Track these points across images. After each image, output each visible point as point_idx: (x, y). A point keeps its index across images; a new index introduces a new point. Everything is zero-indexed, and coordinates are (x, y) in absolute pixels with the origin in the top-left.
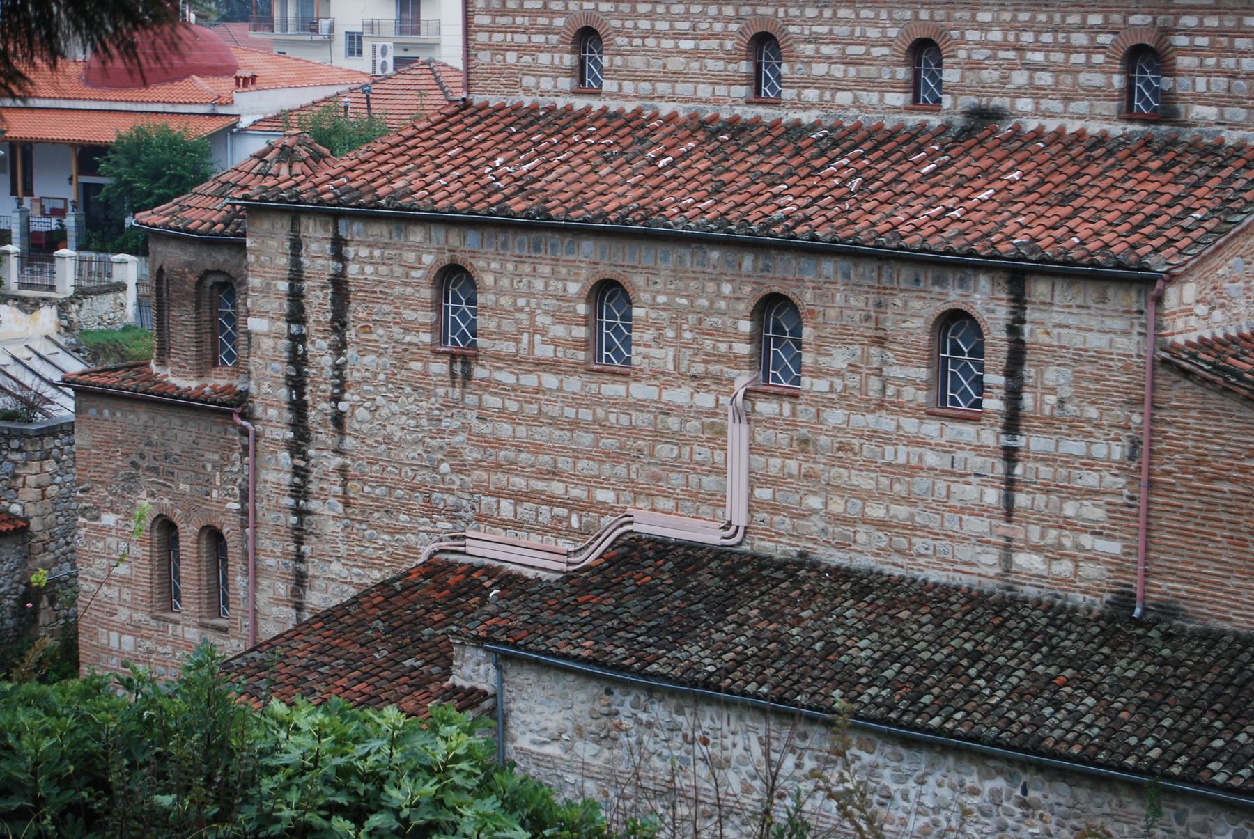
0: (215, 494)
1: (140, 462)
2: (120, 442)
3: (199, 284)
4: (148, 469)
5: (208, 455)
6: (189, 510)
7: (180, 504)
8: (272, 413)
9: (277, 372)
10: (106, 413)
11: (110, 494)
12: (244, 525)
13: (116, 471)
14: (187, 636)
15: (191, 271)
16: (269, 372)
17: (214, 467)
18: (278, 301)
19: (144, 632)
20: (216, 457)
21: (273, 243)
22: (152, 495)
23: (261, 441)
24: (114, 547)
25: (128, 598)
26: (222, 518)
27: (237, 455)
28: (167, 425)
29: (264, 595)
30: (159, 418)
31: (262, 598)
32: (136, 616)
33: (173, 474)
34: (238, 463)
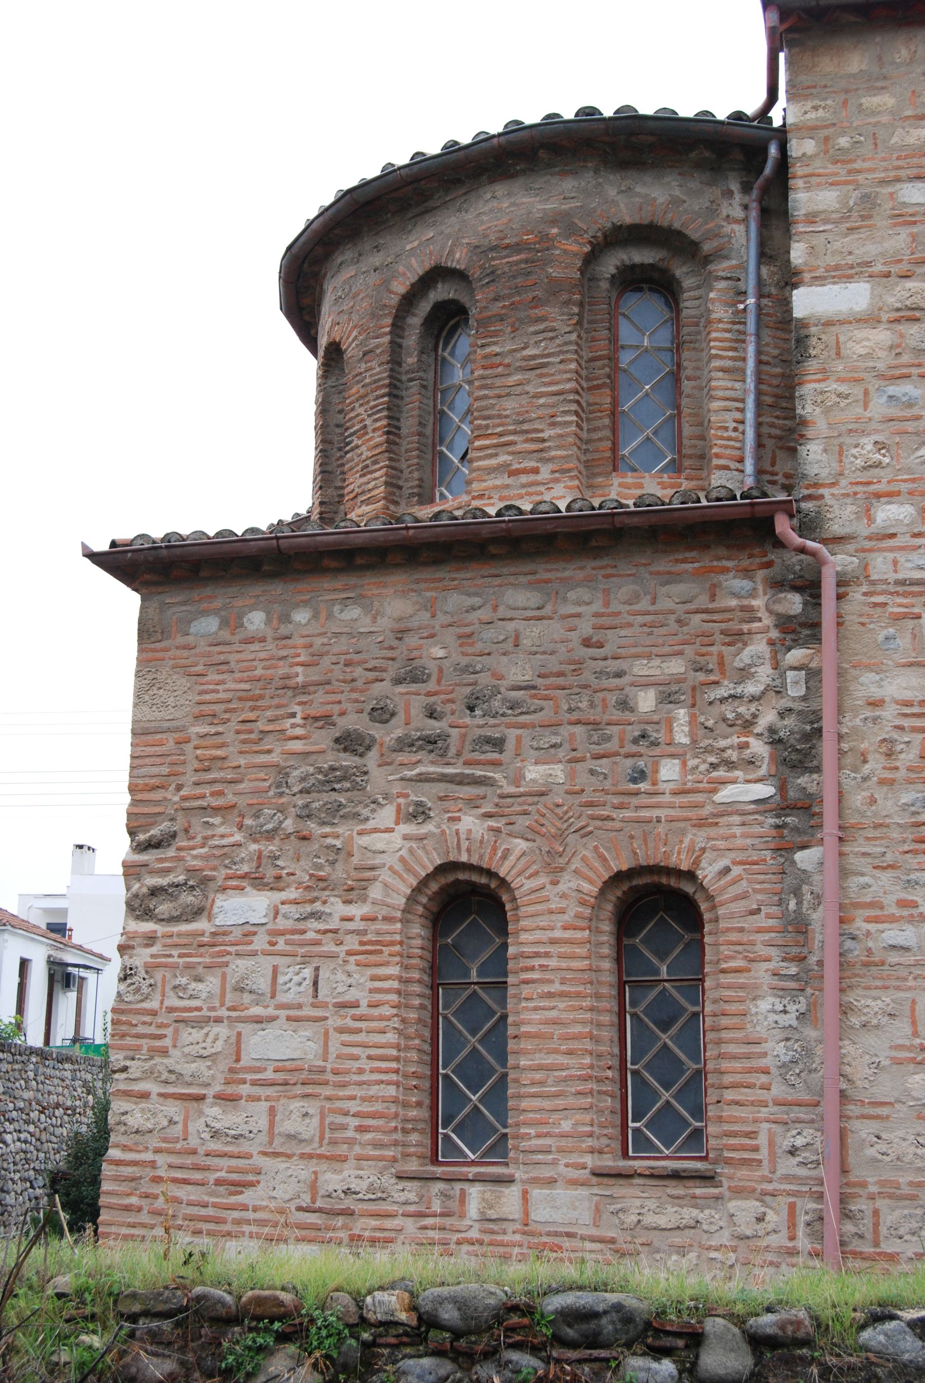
0: (669, 771)
1: (376, 731)
2: (304, 689)
3: (590, 259)
4: (405, 744)
5: (641, 668)
6: (561, 836)
7: (523, 822)
8: (890, 514)
9: (910, 405)
10: (256, 620)
11: (253, 837)
12: (785, 849)
13: (282, 772)
14: (540, 1213)
15: (571, 230)
16: (879, 407)
17: (668, 698)
18: (904, 234)
19: (364, 1226)
20: (676, 667)
21: (885, 100)
22: (419, 813)
23: (856, 595)
24: (263, 984)
25: (309, 1129)
26: (699, 837)
27: (758, 647)
28: (484, 614)
29: (869, 1040)
30: (455, 601)
31: (866, 1054)
32: (332, 1181)
33: (498, 744)
34: (764, 673)
